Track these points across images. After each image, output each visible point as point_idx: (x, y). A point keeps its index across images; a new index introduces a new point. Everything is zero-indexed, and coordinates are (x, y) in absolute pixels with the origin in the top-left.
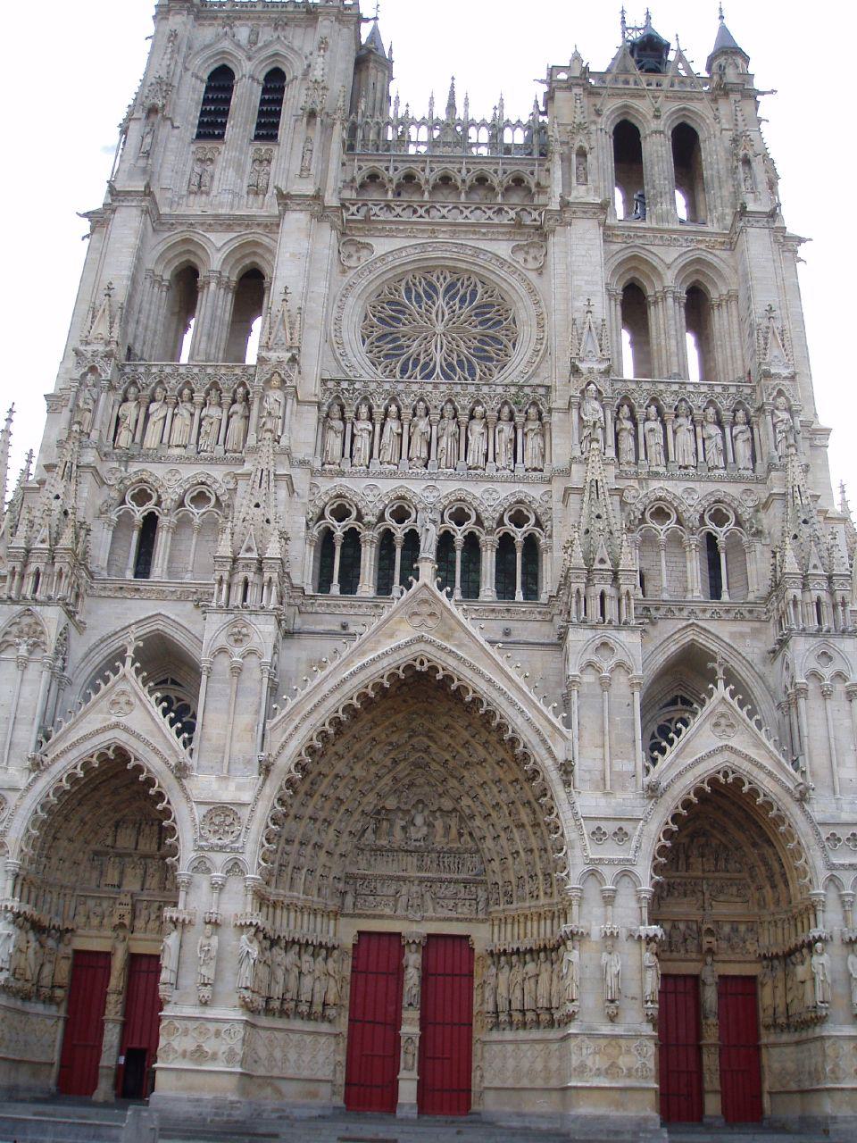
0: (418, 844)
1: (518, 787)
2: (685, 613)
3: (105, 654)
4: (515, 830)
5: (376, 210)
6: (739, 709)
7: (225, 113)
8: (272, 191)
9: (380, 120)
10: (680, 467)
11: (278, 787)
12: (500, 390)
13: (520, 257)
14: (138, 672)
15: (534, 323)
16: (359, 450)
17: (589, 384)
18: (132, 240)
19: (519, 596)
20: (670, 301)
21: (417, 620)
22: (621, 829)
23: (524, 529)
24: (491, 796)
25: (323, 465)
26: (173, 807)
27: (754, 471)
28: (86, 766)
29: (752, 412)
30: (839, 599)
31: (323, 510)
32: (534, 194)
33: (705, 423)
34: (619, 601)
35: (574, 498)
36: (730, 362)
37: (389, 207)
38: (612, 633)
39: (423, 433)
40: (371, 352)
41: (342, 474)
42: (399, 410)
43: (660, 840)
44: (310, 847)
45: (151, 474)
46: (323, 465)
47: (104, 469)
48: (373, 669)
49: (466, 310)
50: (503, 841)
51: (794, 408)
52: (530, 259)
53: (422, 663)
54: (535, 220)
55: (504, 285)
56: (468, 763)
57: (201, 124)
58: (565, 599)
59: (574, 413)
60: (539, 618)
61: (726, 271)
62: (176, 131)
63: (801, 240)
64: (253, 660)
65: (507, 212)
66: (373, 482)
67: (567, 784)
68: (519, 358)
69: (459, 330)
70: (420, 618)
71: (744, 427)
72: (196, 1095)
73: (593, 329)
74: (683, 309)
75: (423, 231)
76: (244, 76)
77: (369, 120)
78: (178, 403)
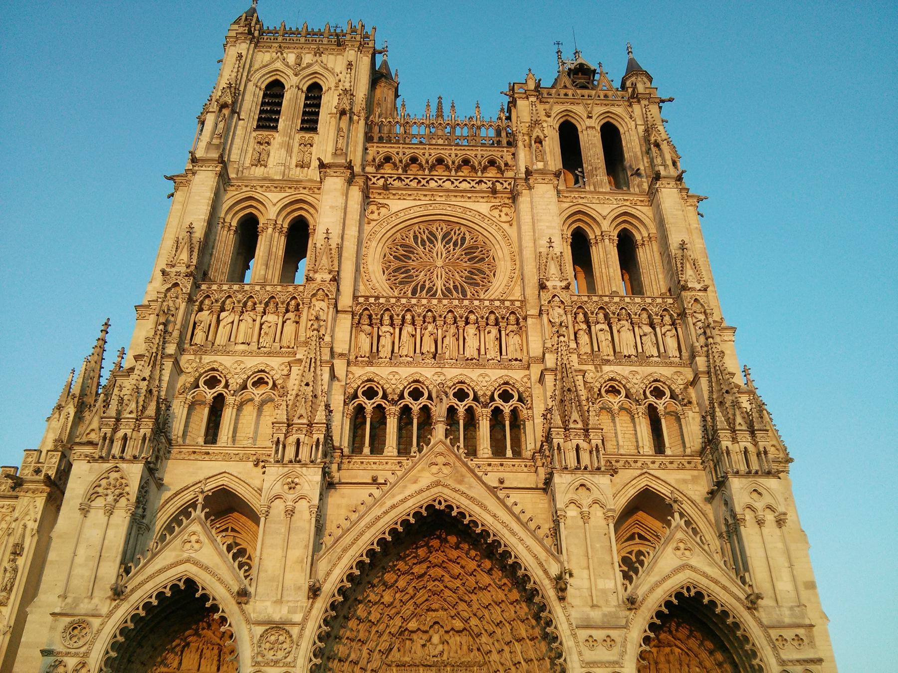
0: (436, 659)
1: (518, 607)
2: (639, 464)
3: (179, 505)
4: (516, 643)
6: (693, 536)
7: (278, 112)
8: (315, 163)
9: (391, 120)
10: (625, 356)
11: (323, 609)
12: (487, 303)
13: (496, 213)
14: (207, 518)
15: (508, 258)
16: (383, 346)
17: (554, 296)
18: (209, 195)
19: (509, 453)
20: (607, 241)
21: (434, 469)
22: (608, 636)
23: (510, 403)
24: (496, 614)
25: (357, 357)
26: (234, 629)
27: (680, 357)
28: (160, 595)
29: (675, 315)
30: (762, 449)
31: (356, 391)
32: (504, 171)
33: (640, 325)
34: (591, 452)
35: (549, 378)
36: (654, 283)
37: (399, 179)
38: (589, 476)
40: (389, 280)
41: (370, 363)
43: (641, 646)
44: (347, 663)
45: (221, 364)
46: (357, 357)
48: (400, 509)
49: (458, 251)
50: (506, 654)
51: (708, 311)
53: (440, 503)
54: (506, 188)
55: (485, 233)
56: (475, 588)
57: (260, 119)
58: (547, 453)
59: (545, 316)
60: (525, 469)
61: (647, 221)
62: (241, 122)
63: (700, 199)
64: (303, 505)
65: (485, 183)
66: (395, 369)
67: (562, 599)
68: (499, 283)
69: (454, 265)
70: (437, 467)
71: (670, 327)
73: (555, 259)
74: (616, 248)
75: (425, 195)
76: (292, 86)
77: (384, 120)
78: (242, 312)
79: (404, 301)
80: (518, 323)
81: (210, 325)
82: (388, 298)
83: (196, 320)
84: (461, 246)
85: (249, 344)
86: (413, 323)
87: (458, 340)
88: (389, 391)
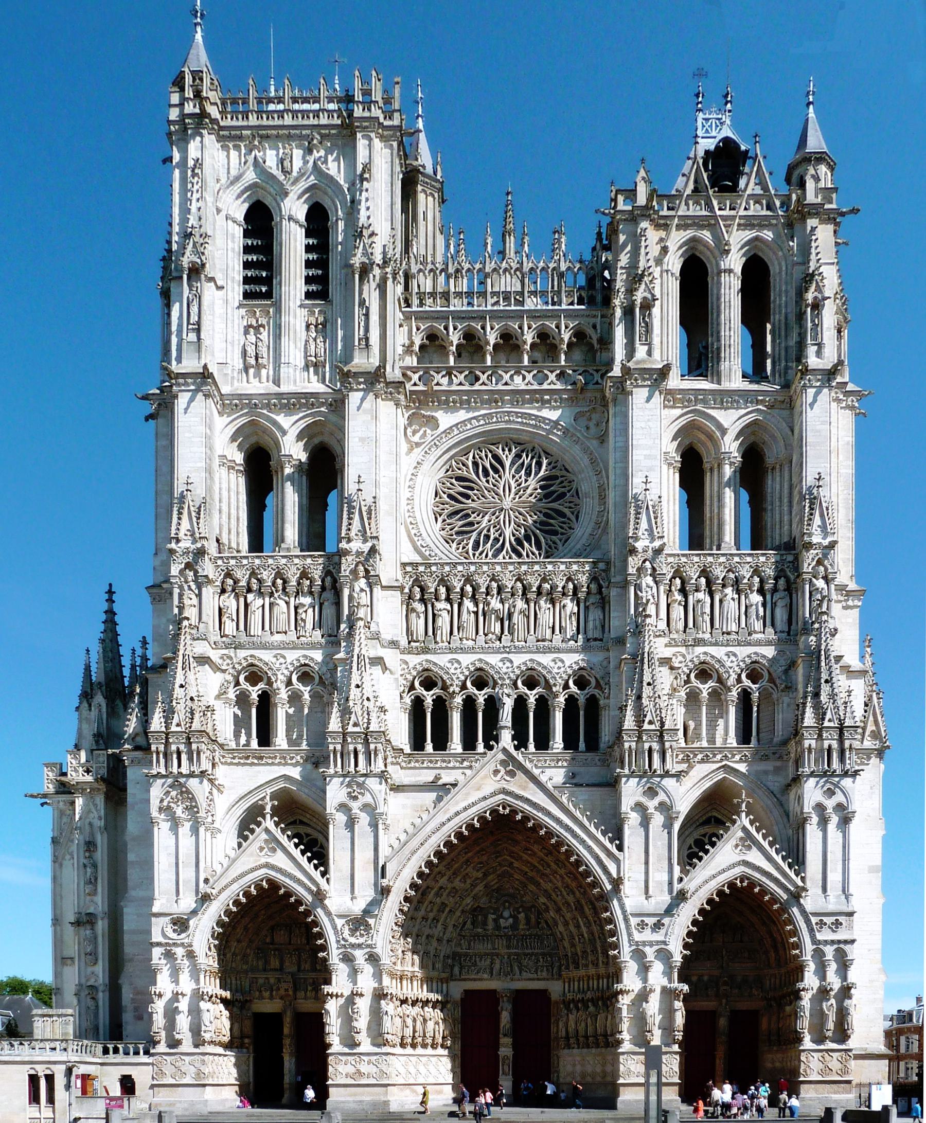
5: (438, 378)
23: (586, 691)
27: (789, 633)
29: (792, 577)
32: (597, 351)
39: (496, 611)
41: (425, 650)
42: (474, 589)
45: (261, 660)
46: (409, 643)
47: (215, 655)
52: (591, 424)
54: (597, 383)
68: (582, 530)
72: (358, 1098)
78: (272, 592)
79: (460, 568)
80: (600, 592)
81: (238, 610)
82: (442, 565)
83: (222, 606)
84: (536, 474)
85: (286, 633)
86: (474, 598)
87: (528, 617)
88: (449, 683)
